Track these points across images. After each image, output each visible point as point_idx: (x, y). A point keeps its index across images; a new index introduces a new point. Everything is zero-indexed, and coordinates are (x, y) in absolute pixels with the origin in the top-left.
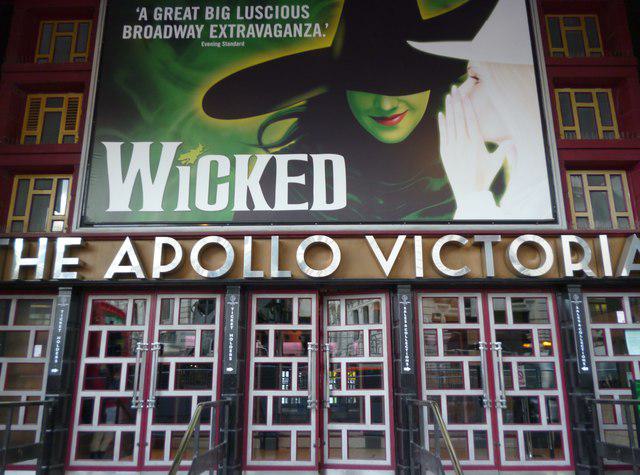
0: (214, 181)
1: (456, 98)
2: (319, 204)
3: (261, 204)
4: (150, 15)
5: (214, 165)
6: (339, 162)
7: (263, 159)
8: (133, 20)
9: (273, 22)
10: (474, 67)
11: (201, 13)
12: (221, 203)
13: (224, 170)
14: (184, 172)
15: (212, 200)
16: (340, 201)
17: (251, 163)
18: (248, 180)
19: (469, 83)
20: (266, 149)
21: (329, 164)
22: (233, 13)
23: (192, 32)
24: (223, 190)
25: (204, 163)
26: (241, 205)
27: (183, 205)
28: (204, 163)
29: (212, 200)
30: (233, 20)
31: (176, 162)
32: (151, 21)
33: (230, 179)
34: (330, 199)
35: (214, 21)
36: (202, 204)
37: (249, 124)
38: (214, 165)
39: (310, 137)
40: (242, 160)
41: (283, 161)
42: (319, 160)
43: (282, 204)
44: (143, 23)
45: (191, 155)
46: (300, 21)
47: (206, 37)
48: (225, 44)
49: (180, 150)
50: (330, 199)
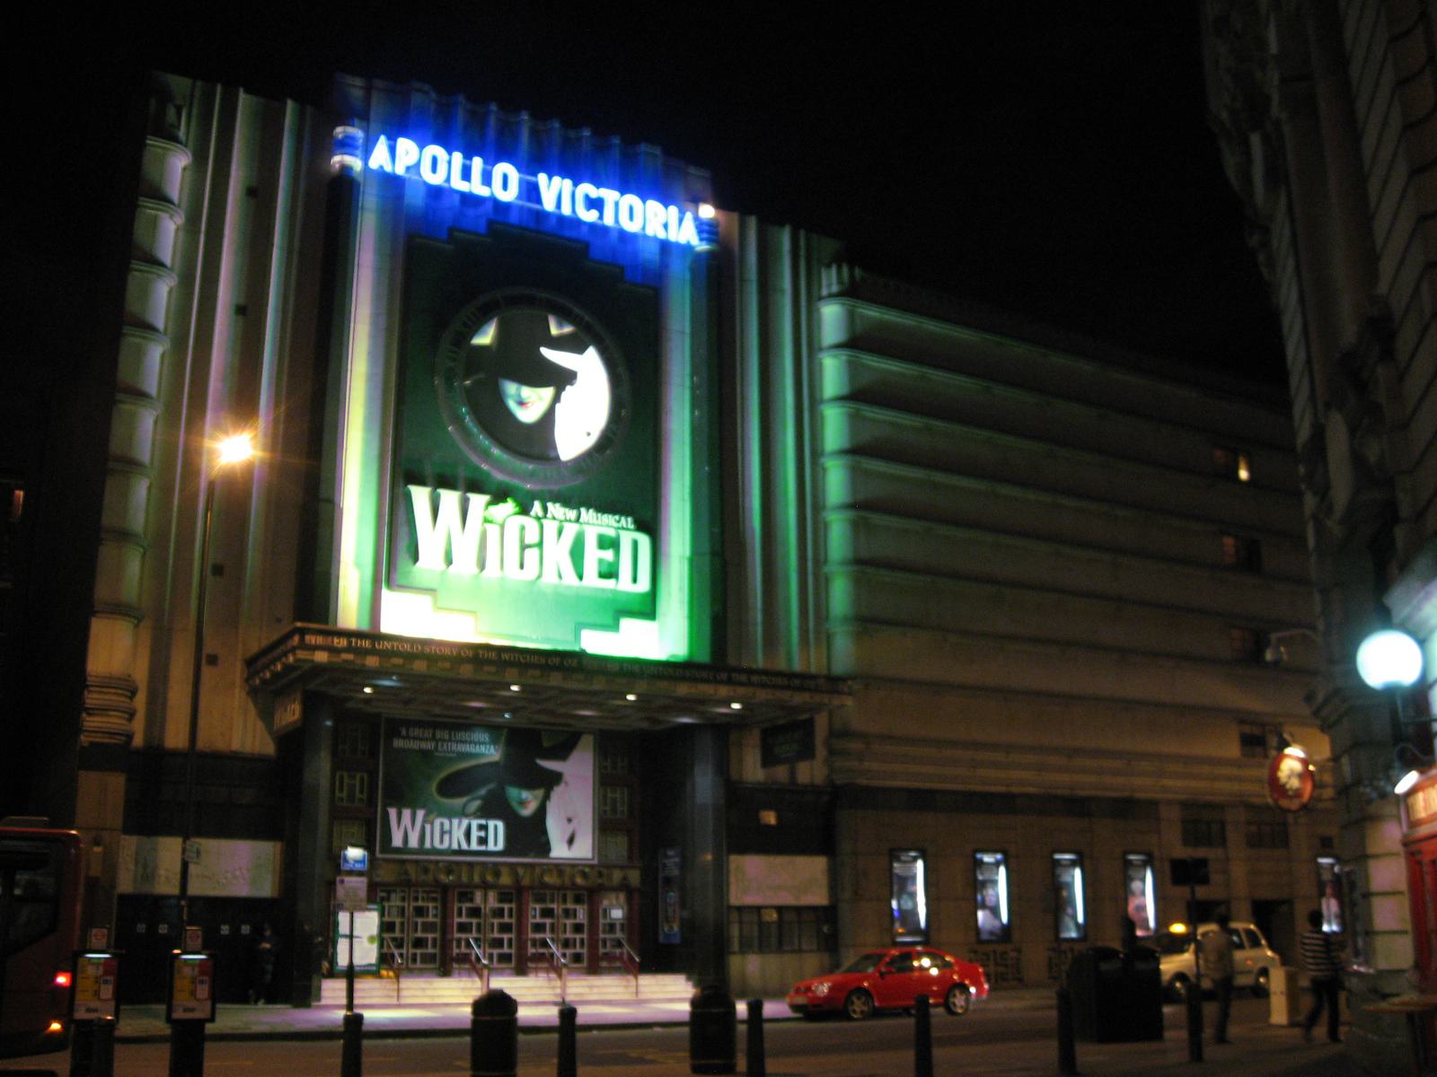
0: (443, 833)
1: (557, 793)
2: (491, 847)
3: (464, 846)
4: (407, 733)
5: (442, 824)
6: (500, 825)
7: (465, 822)
8: (399, 736)
9: (470, 743)
10: (567, 775)
11: (434, 735)
12: (446, 845)
13: (447, 827)
14: (428, 827)
15: (442, 841)
16: (501, 846)
18: (459, 834)
19: (563, 785)
22: (450, 736)
23: (429, 746)
24: (446, 837)
25: (437, 822)
26: (455, 846)
27: (427, 845)
28: (437, 822)
29: (442, 841)
30: (450, 740)
31: (424, 821)
32: (408, 737)
33: (450, 832)
34: (496, 844)
35: (440, 739)
36: (437, 844)
37: (459, 802)
38: (442, 824)
39: (487, 811)
40: (455, 822)
41: (475, 823)
42: (491, 824)
43: (474, 846)
44: (404, 738)
45: (432, 817)
46: (484, 743)
47: (436, 748)
50: (496, 844)
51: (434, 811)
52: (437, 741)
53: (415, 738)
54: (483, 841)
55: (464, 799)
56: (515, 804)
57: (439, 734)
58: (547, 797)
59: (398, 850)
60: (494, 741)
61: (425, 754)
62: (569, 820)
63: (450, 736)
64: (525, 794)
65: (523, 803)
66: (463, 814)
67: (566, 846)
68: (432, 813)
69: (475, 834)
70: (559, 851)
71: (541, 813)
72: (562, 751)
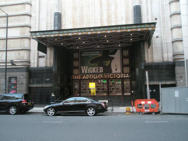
0: (91, 70)
2: (100, 72)
3: (95, 72)
5: (91, 69)
6: (102, 68)
12: (92, 72)
14: (88, 69)
15: (91, 72)
16: (102, 72)
18: (94, 70)
19: (114, 59)
25: (90, 68)
26: (93, 72)
27: (89, 72)
28: (90, 68)
29: (91, 72)
36: (90, 72)
38: (91, 69)
40: (93, 68)
41: (97, 68)
42: (100, 68)
43: (97, 72)
51: (89, 66)
54: (99, 71)
55: (95, 64)
57: (90, 53)
59: (83, 74)
60: (100, 53)
64: (107, 62)
65: (106, 63)
66: (94, 66)
67: (115, 71)
69: (97, 70)
70: (114, 71)
71: (110, 65)
72: (114, 53)
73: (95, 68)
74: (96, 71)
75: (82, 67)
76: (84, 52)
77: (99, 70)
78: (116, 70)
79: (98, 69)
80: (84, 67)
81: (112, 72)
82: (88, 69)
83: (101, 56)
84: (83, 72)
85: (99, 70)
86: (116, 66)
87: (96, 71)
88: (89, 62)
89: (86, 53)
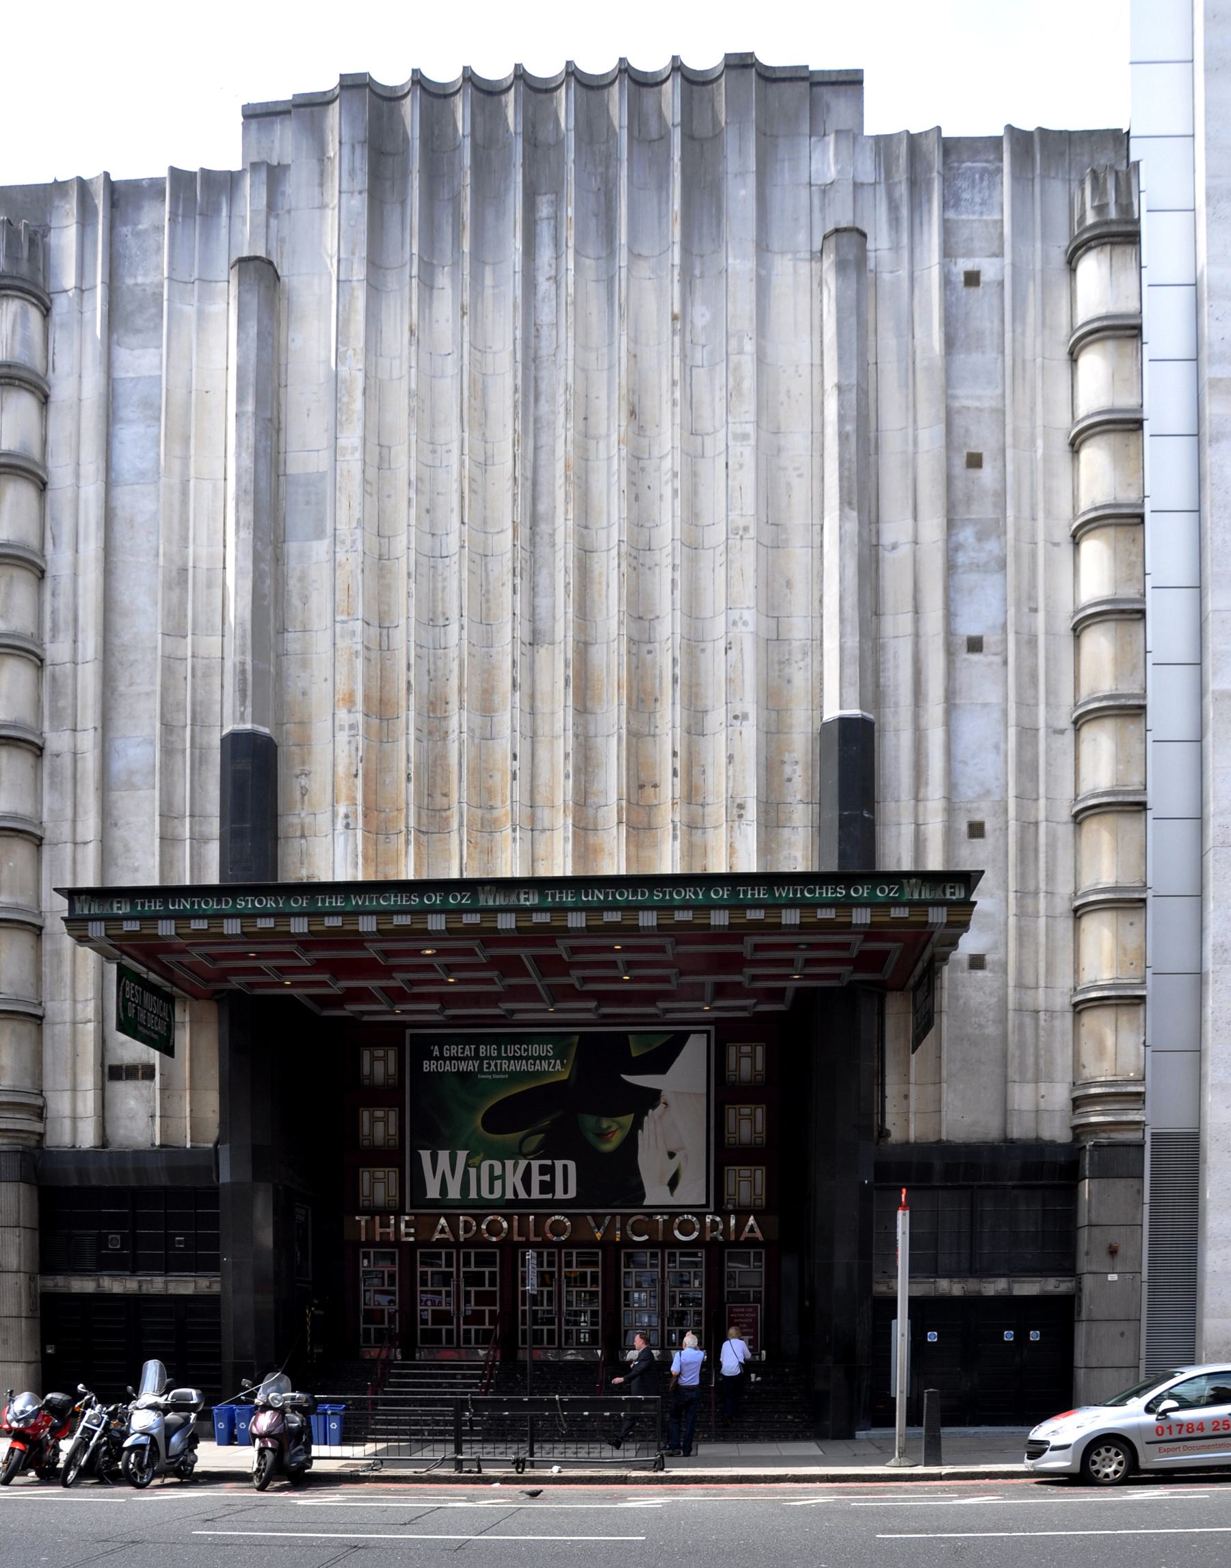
0: (492, 1179)
1: (652, 1119)
2: (559, 1195)
3: (522, 1195)
4: (441, 1052)
5: (491, 1167)
6: (572, 1165)
7: (523, 1164)
8: (430, 1057)
9: (527, 1058)
11: (477, 1050)
12: (497, 1194)
13: (498, 1172)
14: (473, 1171)
15: (491, 1191)
16: (572, 1193)
17: (516, 1166)
18: (514, 1179)
19: (661, 1107)
20: (525, 1156)
21: (565, 1167)
22: (499, 1050)
23: (471, 1066)
24: (498, 1184)
25: (485, 1165)
26: (509, 1195)
28: (485, 1165)
29: (491, 1191)
30: (499, 1057)
31: (467, 1165)
32: (442, 1057)
33: (502, 1177)
35: (486, 1058)
36: (485, 1194)
38: (491, 1167)
40: (509, 1164)
41: (536, 1164)
42: (559, 1164)
43: (536, 1194)
44: (437, 1059)
45: (476, 1160)
46: (546, 1058)
48: (495, 1076)
49: (468, 1157)
52: (481, 1060)
53: (451, 1058)
54: (547, 1187)
55: (519, 1135)
56: (591, 1137)
58: (638, 1124)
59: (434, 1203)
60: (560, 1055)
61: (463, 1076)
62: (671, 1155)
63: (499, 1050)
64: (605, 1123)
65: (603, 1135)
66: (518, 1153)
68: (478, 1154)
70: (656, 1194)
71: (630, 1145)
73: (523, 1164)
74: (528, 1190)
75: (425, 1155)
76: (442, 1040)
77: (547, 1178)
78: (673, 1183)
79: (544, 1170)
80: (444, 1156)
81: (643, 1196)
82: (466, 1174)
83: (565, 1077)
84: (433, 1192)
85: (547, 1178)
86: (671, 1155)
87: (528, 1190)
88: (479, 1122)
89: (454, 1050)
